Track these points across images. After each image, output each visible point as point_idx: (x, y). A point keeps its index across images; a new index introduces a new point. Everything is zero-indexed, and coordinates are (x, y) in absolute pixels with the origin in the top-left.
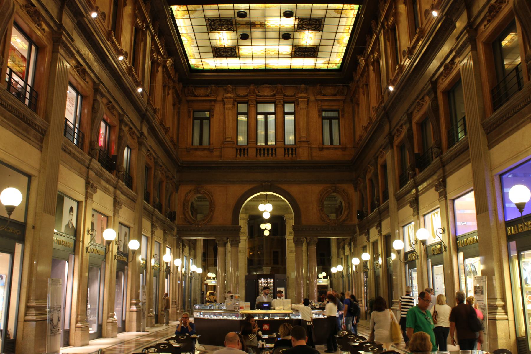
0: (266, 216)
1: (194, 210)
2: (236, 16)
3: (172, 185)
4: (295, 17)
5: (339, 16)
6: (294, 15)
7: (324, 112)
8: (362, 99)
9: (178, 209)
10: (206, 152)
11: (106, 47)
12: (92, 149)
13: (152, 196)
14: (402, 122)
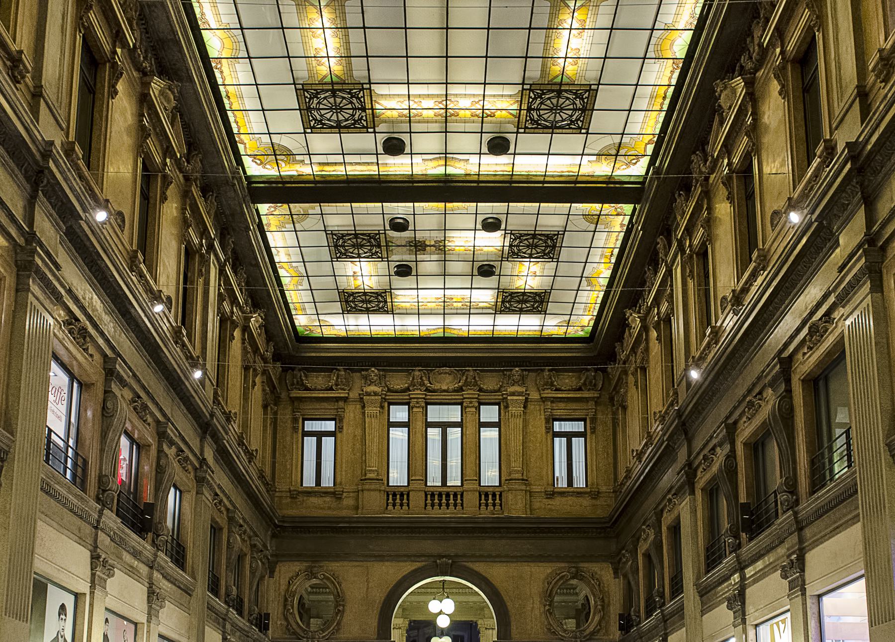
0: (443, 622)
1: (305, 611)
2: (388, 227)
3: (263, 563)
4: (505, 230)
5: (592, 227)
6: (503, 227)
7: (556, 424)
8: (633, 397)
9: (274, 609)
10: (328, 499)
11: (129, 284)
12: (104, 491)
13: (223, 583)
14: (714, 441)
